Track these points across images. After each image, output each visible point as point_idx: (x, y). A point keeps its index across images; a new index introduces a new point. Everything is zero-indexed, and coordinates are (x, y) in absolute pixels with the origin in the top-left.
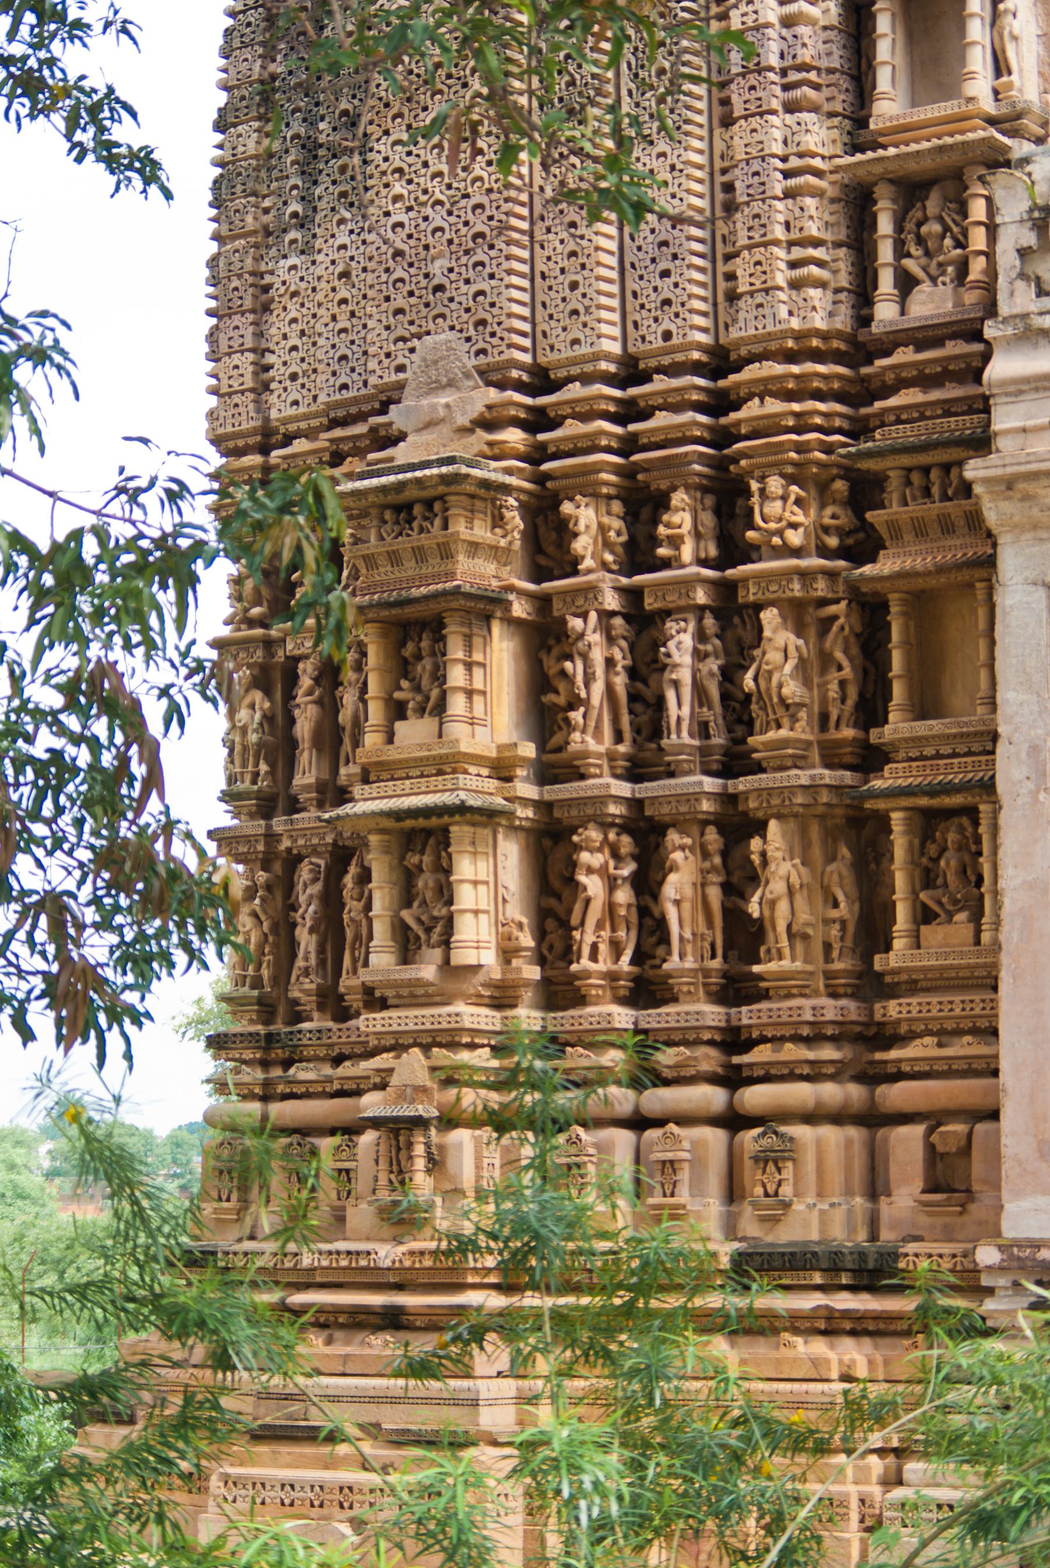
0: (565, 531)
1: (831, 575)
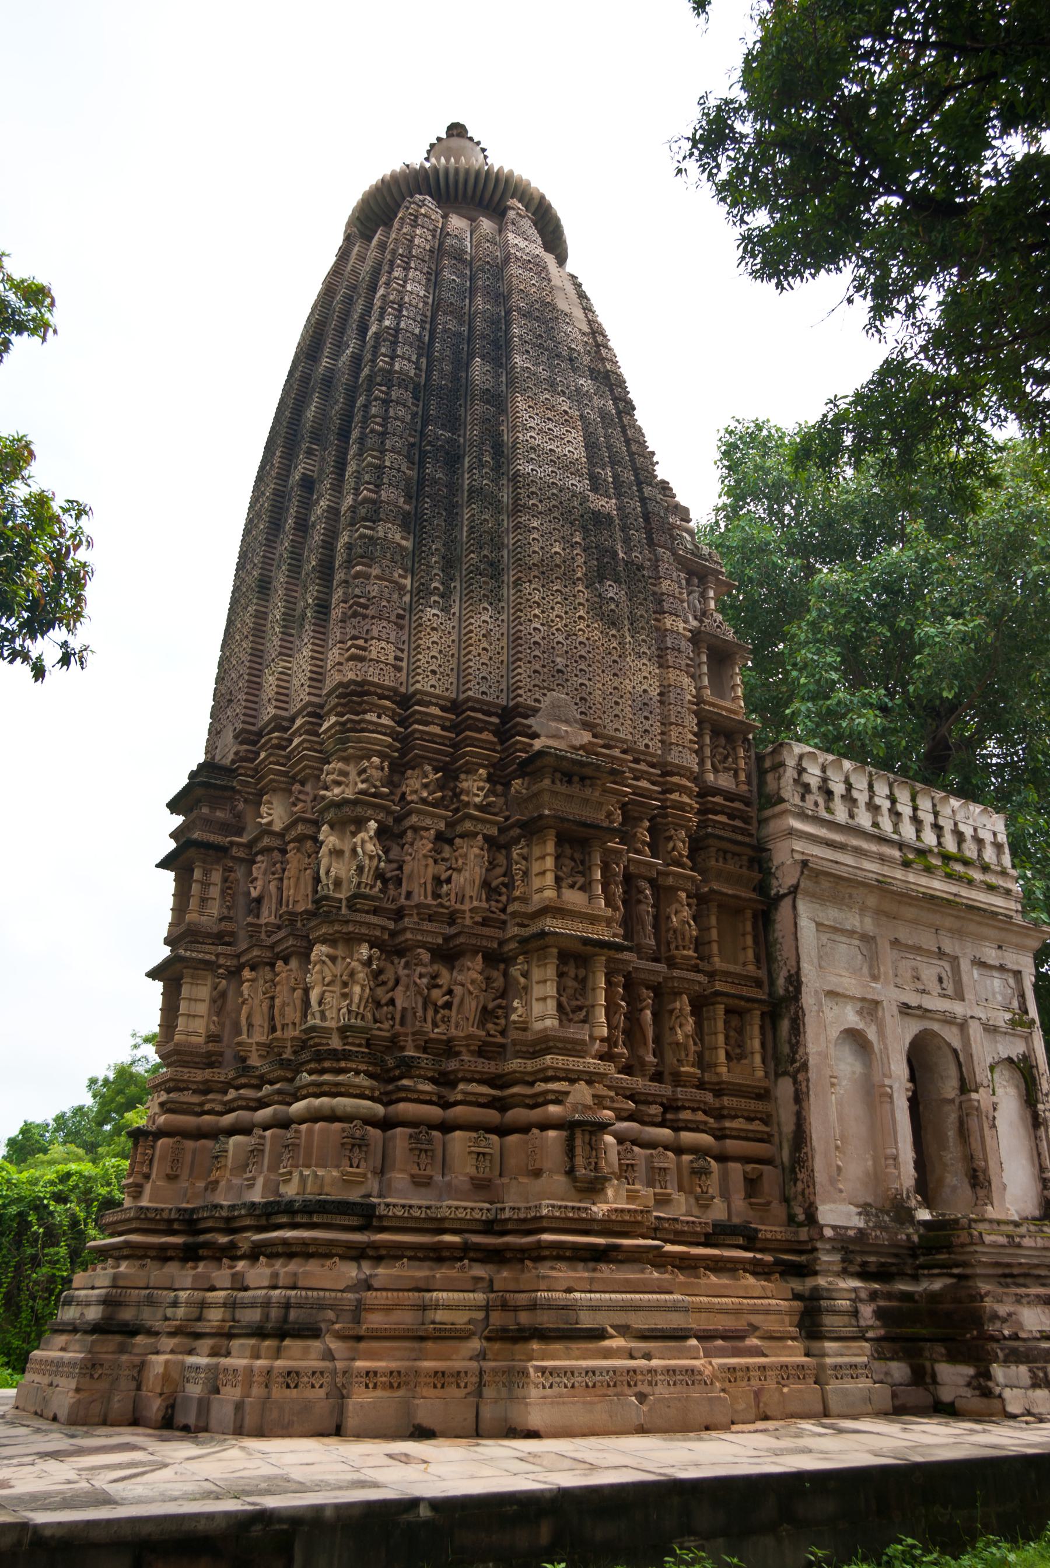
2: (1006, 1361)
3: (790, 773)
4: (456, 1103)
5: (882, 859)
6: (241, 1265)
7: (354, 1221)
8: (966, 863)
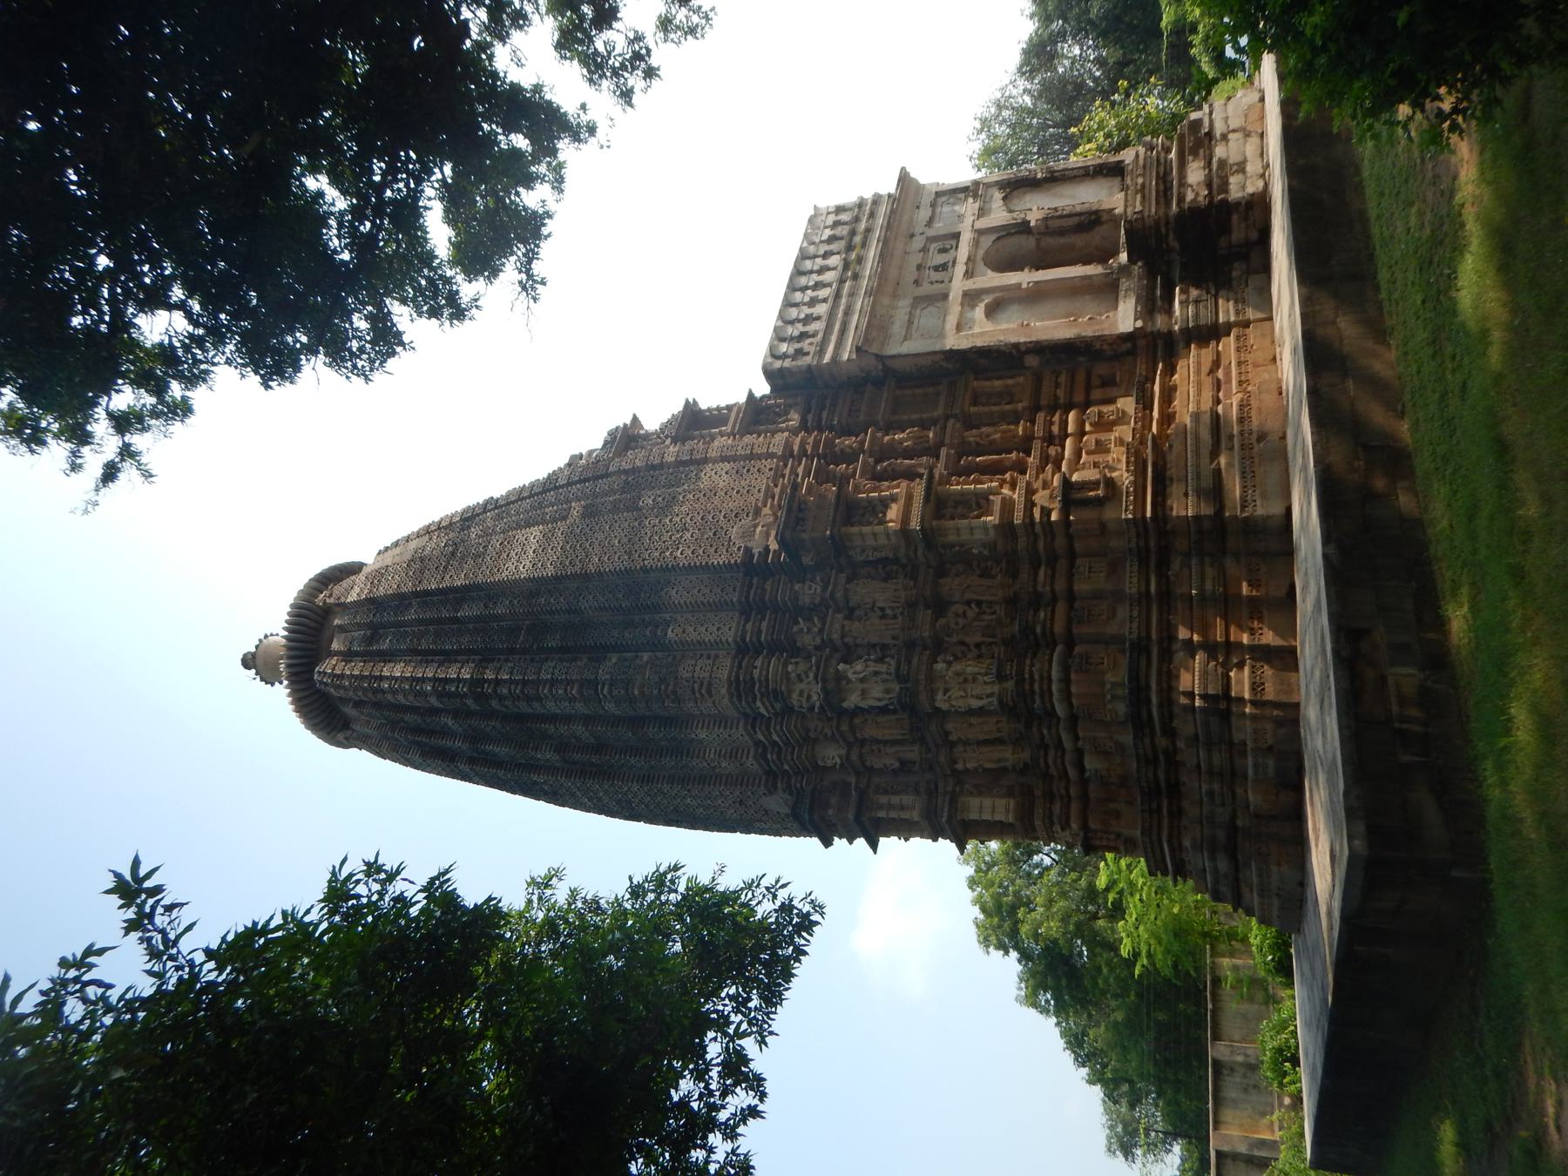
2: (1227, 191)
3: (787, 363)
4: (1053, 591)
5: (852, 295)
6: (1181, 744)
7: (1143, 658)
8: (853, 233)
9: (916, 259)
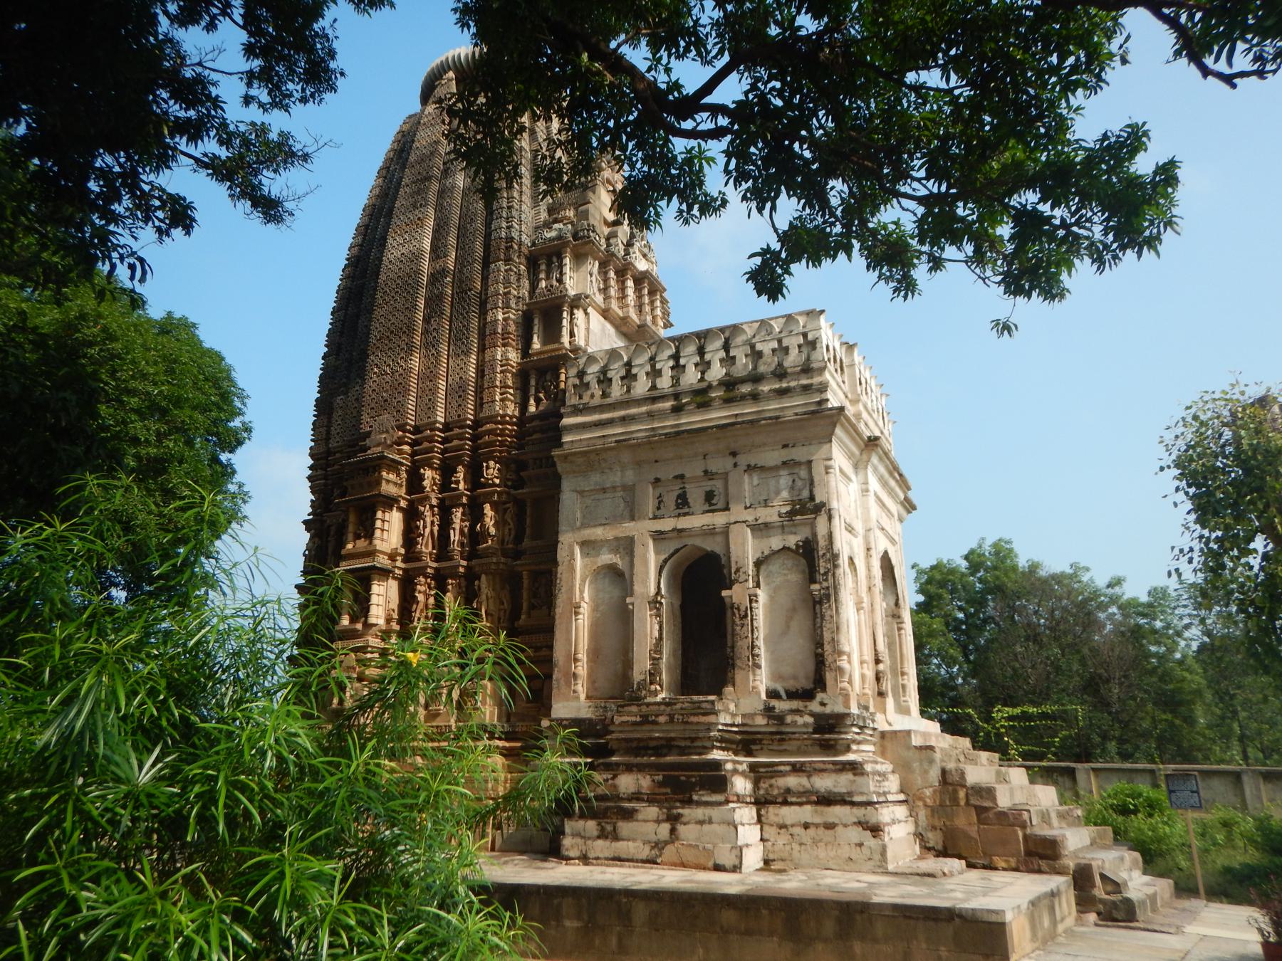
0: (422, 478)
1: (508, 493)
9: (693, 469)
